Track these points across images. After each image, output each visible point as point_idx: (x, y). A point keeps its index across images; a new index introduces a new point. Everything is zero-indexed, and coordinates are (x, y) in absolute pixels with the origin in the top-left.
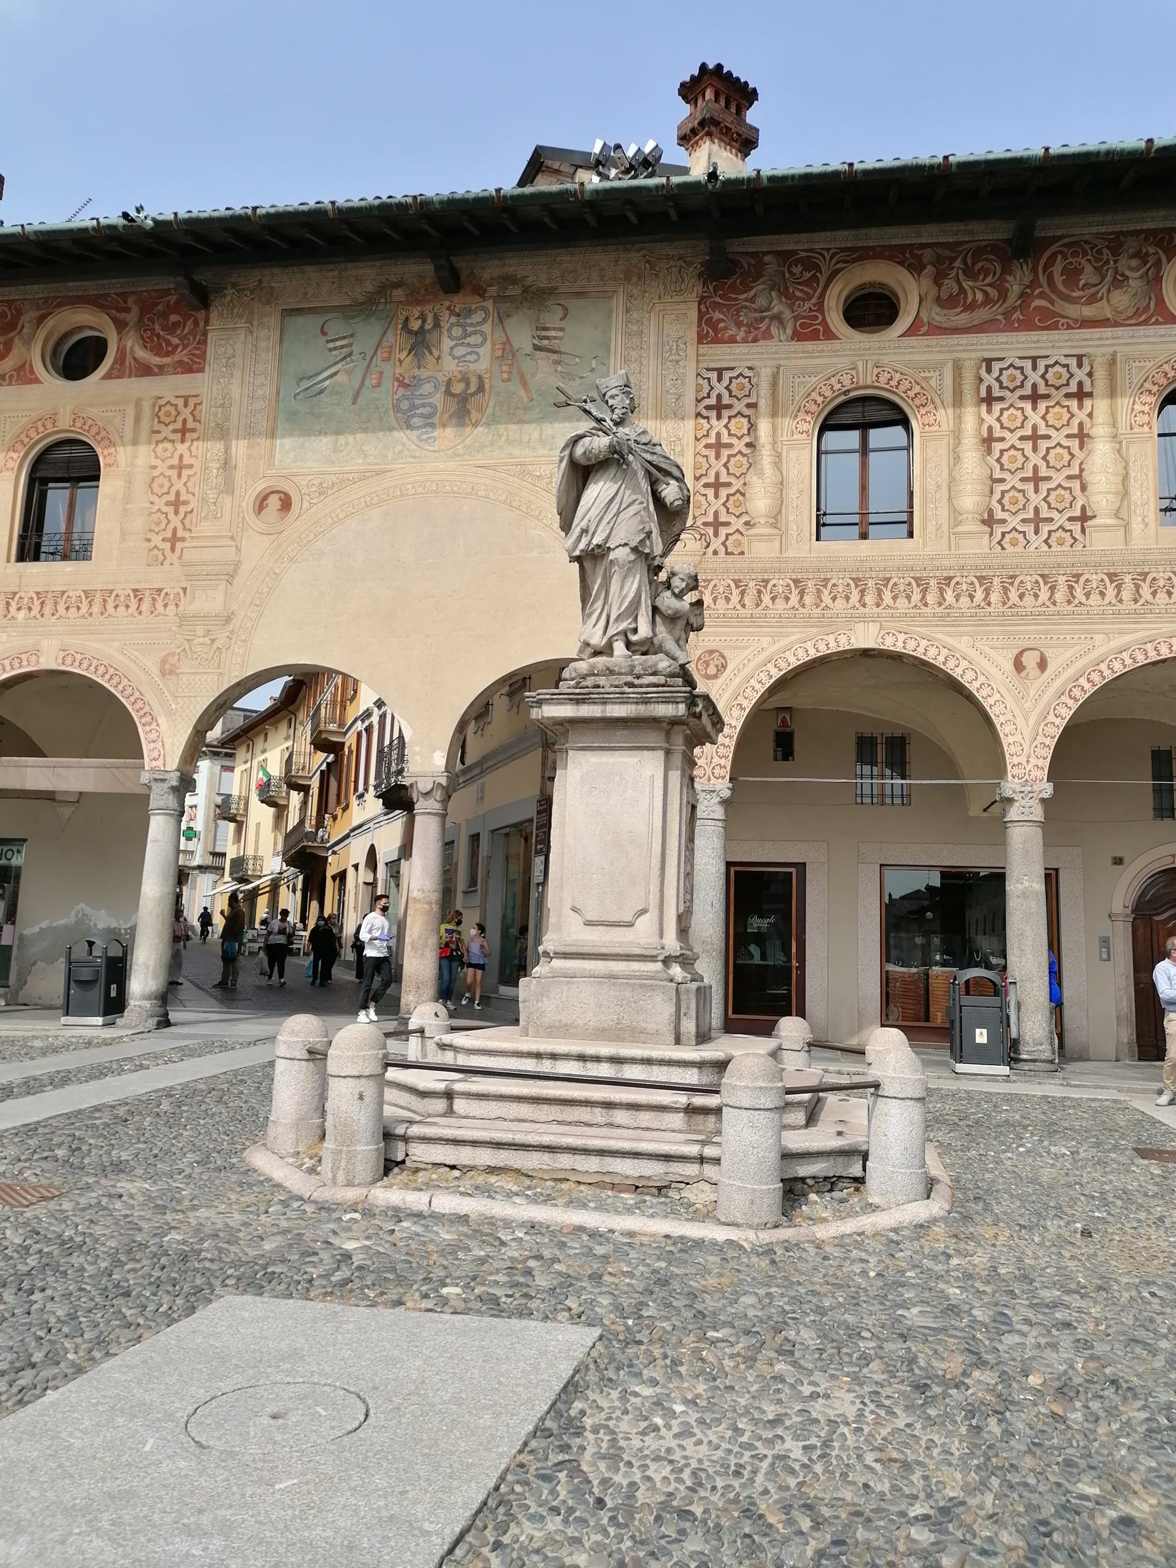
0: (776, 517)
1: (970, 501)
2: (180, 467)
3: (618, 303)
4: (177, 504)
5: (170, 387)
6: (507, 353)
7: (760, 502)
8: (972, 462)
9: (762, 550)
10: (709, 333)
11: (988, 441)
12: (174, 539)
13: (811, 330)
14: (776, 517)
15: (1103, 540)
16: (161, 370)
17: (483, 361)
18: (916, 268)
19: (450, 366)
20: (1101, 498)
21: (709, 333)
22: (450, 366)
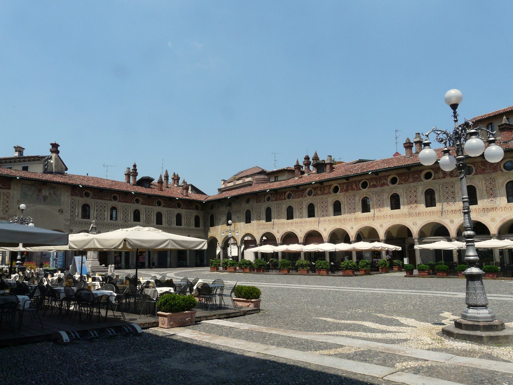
0: (78, 216)
1: (95, 216)
2: (7, 202)
3: (63, 190)
4: (7, 207)
5: (6, 191)
6: (50, 193)
7: (76, 214)
8: (95, 213)
9: (76, 219)
10: (72, 195)
11: (97, 210)
12: (7, 211)
13: (82, 196)
14: (78, 216)
15: (106, 221)
16: (4, 188)
17: (47, 194)
18: (91, 191)
19: (43, 194)
20: (106, 217)
21: (72, 195)
22: (43, 194)
